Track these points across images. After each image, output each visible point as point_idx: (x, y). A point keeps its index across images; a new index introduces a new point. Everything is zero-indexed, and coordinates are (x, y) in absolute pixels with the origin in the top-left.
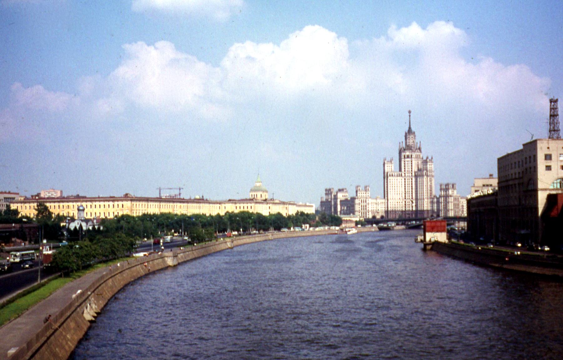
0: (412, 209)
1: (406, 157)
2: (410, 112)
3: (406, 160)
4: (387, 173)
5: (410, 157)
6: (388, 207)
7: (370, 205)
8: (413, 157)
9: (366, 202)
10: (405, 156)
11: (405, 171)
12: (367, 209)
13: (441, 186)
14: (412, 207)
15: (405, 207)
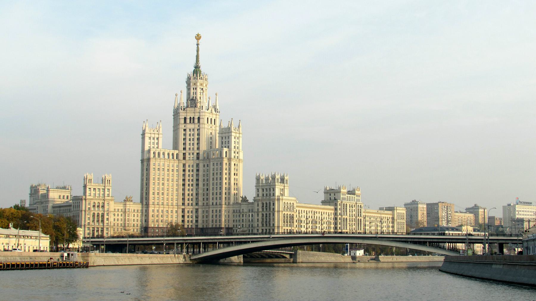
0: (197, 226)
1: (188, 121)
2: (198, 37)
3: (190, 126)
4: (149, 151)
5: (196, 121)
6: (147, 221)
7: (111, 215)
8: (201, 121)
9: (103, 207)
10: (185, 119)
11: (184, 149)
12: (106, 222)
13: (258, 179)
14: (197, 221)
15: (183, 221)
